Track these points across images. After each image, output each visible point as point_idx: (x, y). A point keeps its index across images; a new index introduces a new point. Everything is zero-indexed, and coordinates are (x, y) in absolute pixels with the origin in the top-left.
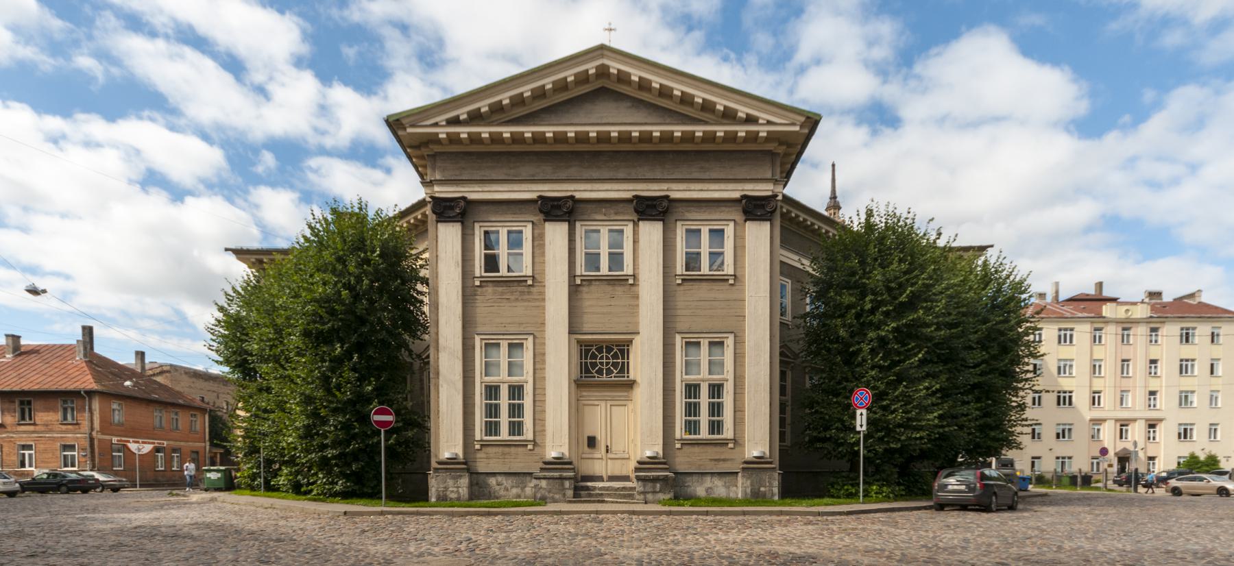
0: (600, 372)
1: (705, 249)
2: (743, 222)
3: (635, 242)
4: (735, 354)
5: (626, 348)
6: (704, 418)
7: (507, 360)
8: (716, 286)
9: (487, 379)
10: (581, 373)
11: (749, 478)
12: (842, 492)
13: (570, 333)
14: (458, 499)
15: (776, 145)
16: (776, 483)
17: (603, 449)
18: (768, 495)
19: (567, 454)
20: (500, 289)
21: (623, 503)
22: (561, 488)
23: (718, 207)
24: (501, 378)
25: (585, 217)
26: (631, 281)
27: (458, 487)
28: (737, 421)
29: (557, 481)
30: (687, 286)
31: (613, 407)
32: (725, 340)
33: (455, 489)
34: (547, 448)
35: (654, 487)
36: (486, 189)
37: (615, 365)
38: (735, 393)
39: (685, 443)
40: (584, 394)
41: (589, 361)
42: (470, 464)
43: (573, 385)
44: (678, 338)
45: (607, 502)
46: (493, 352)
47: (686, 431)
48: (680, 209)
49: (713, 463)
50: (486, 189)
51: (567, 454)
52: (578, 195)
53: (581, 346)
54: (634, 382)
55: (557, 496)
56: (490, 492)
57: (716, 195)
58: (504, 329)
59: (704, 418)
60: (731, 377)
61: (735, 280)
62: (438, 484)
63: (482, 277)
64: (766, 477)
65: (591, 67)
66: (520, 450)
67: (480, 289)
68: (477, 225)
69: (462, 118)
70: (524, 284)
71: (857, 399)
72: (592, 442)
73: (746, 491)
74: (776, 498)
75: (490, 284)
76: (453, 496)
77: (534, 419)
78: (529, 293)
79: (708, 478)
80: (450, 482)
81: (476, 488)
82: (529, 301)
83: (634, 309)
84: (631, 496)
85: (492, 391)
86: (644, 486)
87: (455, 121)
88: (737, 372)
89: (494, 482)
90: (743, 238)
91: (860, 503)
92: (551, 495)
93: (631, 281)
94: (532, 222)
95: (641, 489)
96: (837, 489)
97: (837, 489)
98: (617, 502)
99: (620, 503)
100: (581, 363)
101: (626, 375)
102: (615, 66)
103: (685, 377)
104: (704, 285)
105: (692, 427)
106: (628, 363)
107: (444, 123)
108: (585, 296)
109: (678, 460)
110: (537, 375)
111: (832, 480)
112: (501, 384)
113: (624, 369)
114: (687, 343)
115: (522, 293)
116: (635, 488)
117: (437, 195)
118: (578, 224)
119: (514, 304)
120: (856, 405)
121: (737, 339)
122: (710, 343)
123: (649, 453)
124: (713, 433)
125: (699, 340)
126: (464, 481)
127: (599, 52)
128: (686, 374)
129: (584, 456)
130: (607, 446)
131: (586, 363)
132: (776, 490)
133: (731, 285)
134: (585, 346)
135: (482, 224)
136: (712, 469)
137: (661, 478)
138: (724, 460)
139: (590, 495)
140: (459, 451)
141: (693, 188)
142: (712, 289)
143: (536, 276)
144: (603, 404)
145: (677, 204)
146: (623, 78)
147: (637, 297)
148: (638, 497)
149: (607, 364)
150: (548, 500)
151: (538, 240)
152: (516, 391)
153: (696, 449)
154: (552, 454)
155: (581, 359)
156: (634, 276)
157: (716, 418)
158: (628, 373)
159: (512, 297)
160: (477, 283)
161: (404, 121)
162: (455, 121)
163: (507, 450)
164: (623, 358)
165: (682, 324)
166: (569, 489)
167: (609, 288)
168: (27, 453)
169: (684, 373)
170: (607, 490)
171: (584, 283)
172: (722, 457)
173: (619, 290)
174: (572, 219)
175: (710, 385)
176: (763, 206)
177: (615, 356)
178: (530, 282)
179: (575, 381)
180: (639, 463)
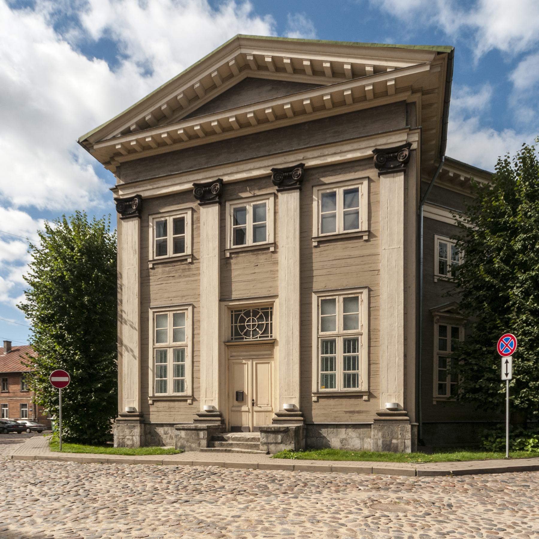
0: (247, 334)
2: (378, 178)
3: (275, 213)
4: (369, 308)
5: (269, 310)
6: (339, 372)
7: (172, 328)
8: (350, 244)
9: (158, 345)
10: (232, 336)
11: (380, 430)
12: (494, 445)
13: (221, 300)
14: (133, 445)
15: (409, 93)
16: (409, 435)
18: (401, 448)
19: (217, 407)
21: (247, 452)
22: (196, 438)
24: (168, 343)
25: (234, 197)
26: (272, 249)
27: (133, 436)
28: (372, 373)
29: (194, 432)
30: (323, 247)
31: (258, 365)
32: (360, 295)
33: (131, 437)
34: (201, 403)
35: (276, 438)
36: (155, 186)
38: (369, 347)
39: (321, 396)
40: (235, 354)
41: (238, 324)
42: (145, 416)
43: (223, 346)
44: (314, 297)
45: (233, 452)
47: (322, 385)
48: (317, 175)
49: (348, 415)
50: (155, 186)
51: (217, 407)
52: (226, 179)
53: (232, 312)
55: (194, 445)
56: (159, 440)
58: (171, 302)
59: (339, 372)
60: (365, 331)
61: (369, 236)
62: (118, 433)
63: (154, 260)
64: (397, 429)
65: (230, 60)
66: (182, 404)
68: (151, 218)
70: (185, 262)
71: (511, 345)
72: (240, 396)
73: (377, 444)
74: (409, 451)
75: (160, 266)
76: (129, 443)
77: (193, 378)
78: (189, 269)
79: (343, 430)
80: (127, 431)
81: (149, 436)
82: (189, 276)
83: (273, 275)
84: (256, 446)
85: (162, 355)
86: (267, 438)
88: (371, 325)
89: (162, 432)
90: (377, 194)
91: (506, 459)
92: (189, 444)
93: (272, 249)
95: (264, 440)
96: (490, 441)
97: (490, 441)
98: (241, 452)
99: (244, 452)
100: (232, 327)
102: (253, 52)
103: (321, 333)
104: (339, 244)
105: (328, 381)
106: (271, 324)
107: (119, 136)
108: (233, 267)
109: (314, 412)
110: (195, 340)
111: (486, 431)
112: (168, 349)
113: (267, 330)
115: (184, 270)
116: (259, 439)
117: (121, 197)
119: (178, 280)
120: (501, 352)
121: (371, 293)
123: (285, 406)
124: (349, 386)
125: (334, 297)
126: (137, 431)
127: (236, 44)
128: (322, 331)
130: (253, 400)
131: (236, 326)
132: (408, 443)
133: (366, 241)
134: (235, 311)
135: (154, 216)
136: (347, 421)
137: (282, 429)
138: (359, 412)
139: (222, 445)
140: (136, 405)
141: (326, 153)
142: (346, 248)
143: (195, 254)
144: (250, 363)
146: (259, 63)
147: (276, 263)
148: (261, 447)
150: (186, 449)
152: (179, 354)
153: (332, 402)
154: (204, 408)
155: (232, 323)
156: (275, 244)
157: (351, 372)
158: (271, 333)
159: (176, 275)
160: (151, 266)
162: (127, 132)
163: (172, 404)
165: (317, 285)
166: (203, 439)
168: (5, 409)
170: (239, 440)
171: (233, 256)
172: (357, 409)
173: (262, 258)
176: (395, 158)
177: (261, 318)
178: (189, 260)
179: (225, 342)
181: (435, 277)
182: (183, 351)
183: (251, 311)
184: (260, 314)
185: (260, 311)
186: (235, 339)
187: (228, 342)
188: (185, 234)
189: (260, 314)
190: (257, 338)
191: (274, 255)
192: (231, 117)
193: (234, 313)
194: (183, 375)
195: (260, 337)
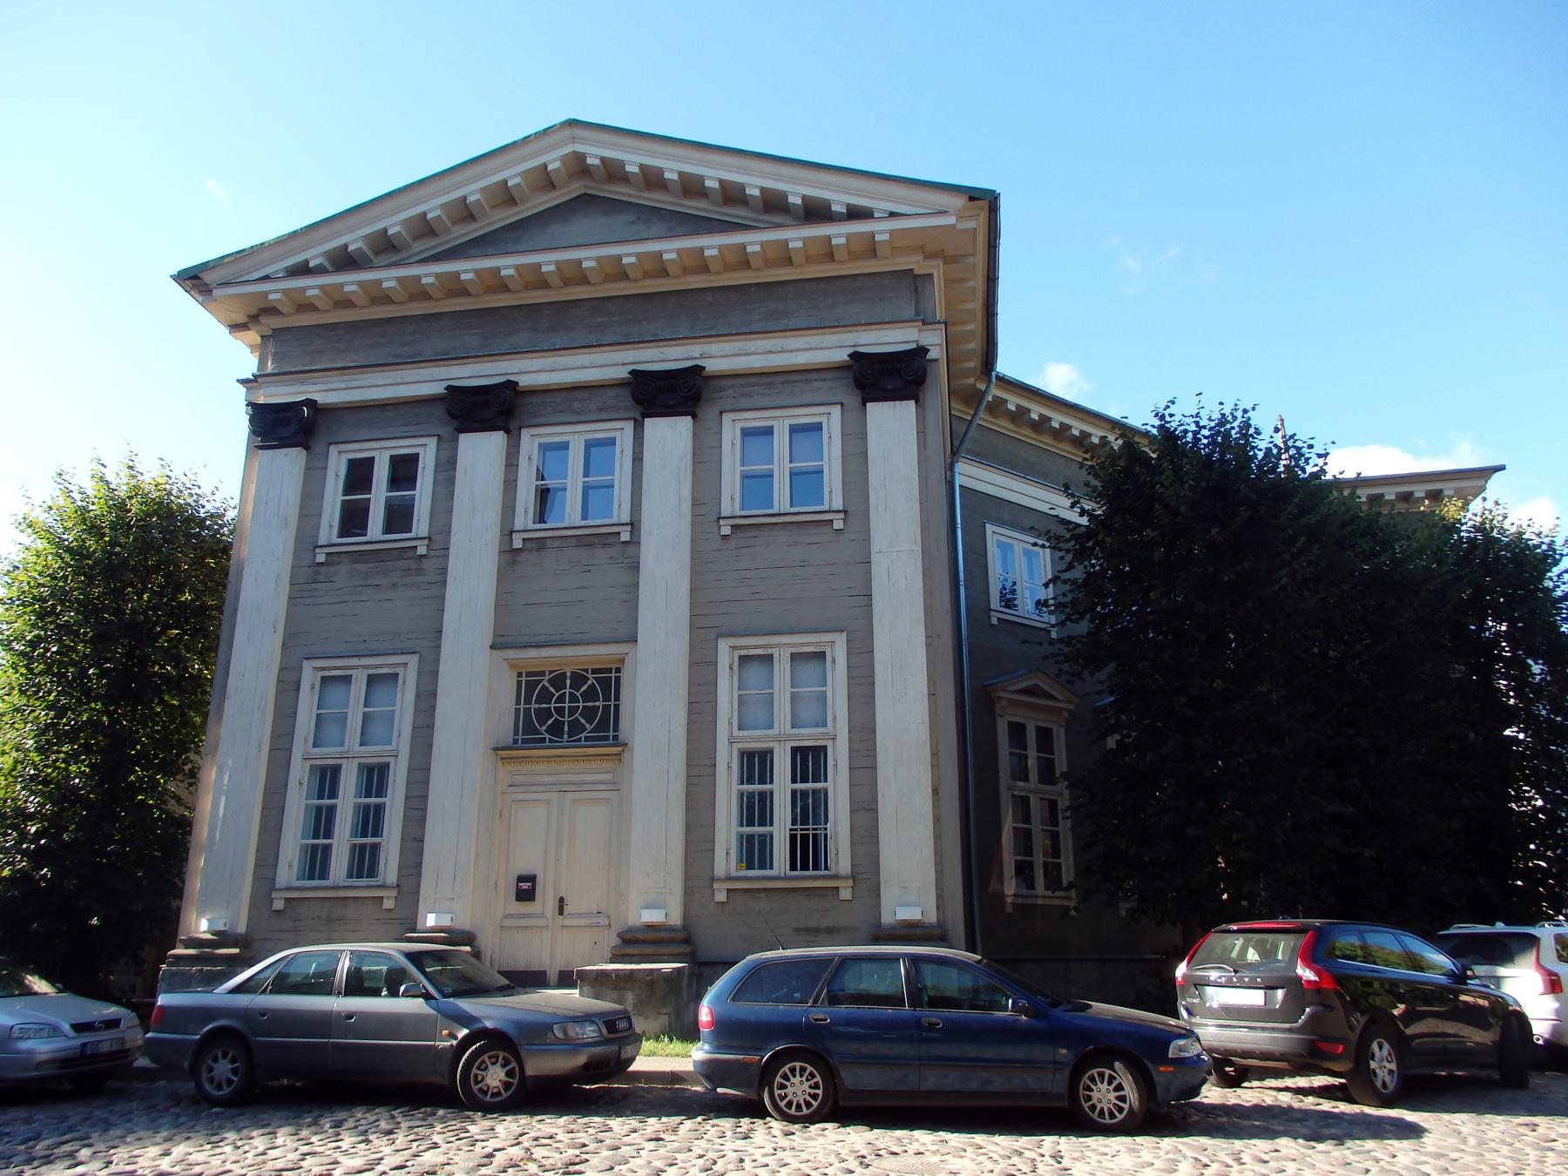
1: (781, 465)
3: (638, 459)
5: (613, 675)
10: (516, 732)
17: (551, 906)
20: (363, 567)
23: (808, 381)
36: (353, 384)
37: (589, 714)
46: (335, 693)
52: (524, 381)
57: (802, 359)
67: (324, 569)
69: (311, 264)
70: (410, 554)
78: (420, 571)
85: (327, 779)
87: (303, 270)
93: (625, 537)
94: (438, 435)
100: (518, 711)
101: (611, 734)
104: (781, 536)
112: (344, 762)
114: (743, 659)
118: (525, 433)
122: (794, 657)
125: (770, 651)
129: (508, 922)
134: (528, 674)
145: (724, 383)
149: (573, 710)
151: (447, 467)
152: (375, 778)
156: (634, 525)
161: (208, 278)
162: (303, 270)
164: (607, 698)
167: (582, 553)
169: (735, 726)
171: (529, 545)
173: (601, 555)
174: (513, 426)
175: (795, 750)
179: (496, 749)
181: (993, 613)
182: (383, 769)
183: (568, 674)
184: (590, 682)
185: (590, 676)
186: (524, 741)
187: (503, 749)
188: (417, 493)
189: (590, 682)
190: (579, 740)
191: (631, 550)
192: (548, 261)
193: (524, 679)
194: (377, 832)
195: (587, 739)
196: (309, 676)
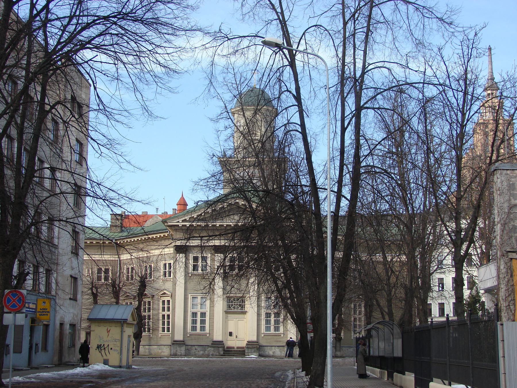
0: (234, 308)
43: (224, 313)
46: (196, 300)
54: (246, 312)
66: (204, 336)
72: (231, 334)
76: (179, 354)
80: (178, 349)
113: (243, 307)
131: (229, 305)
152: (203, 315)
172: (279, 340)
180: (248, 342)
196: (190, 297)
